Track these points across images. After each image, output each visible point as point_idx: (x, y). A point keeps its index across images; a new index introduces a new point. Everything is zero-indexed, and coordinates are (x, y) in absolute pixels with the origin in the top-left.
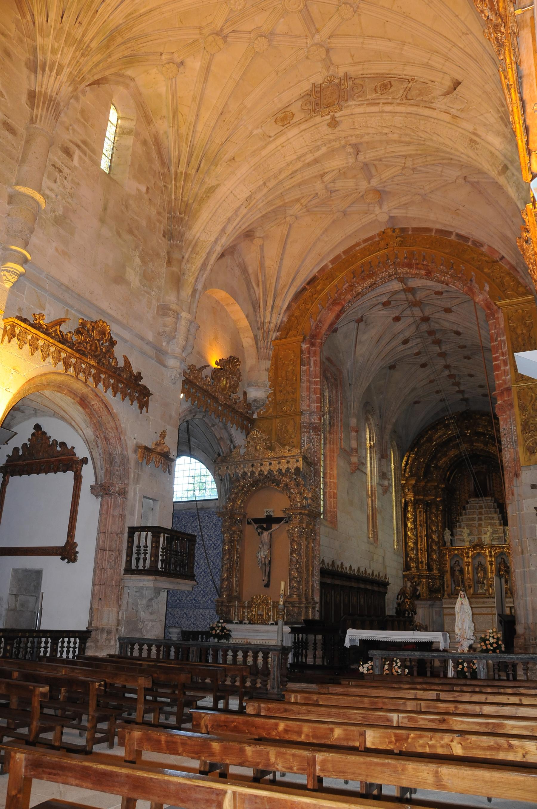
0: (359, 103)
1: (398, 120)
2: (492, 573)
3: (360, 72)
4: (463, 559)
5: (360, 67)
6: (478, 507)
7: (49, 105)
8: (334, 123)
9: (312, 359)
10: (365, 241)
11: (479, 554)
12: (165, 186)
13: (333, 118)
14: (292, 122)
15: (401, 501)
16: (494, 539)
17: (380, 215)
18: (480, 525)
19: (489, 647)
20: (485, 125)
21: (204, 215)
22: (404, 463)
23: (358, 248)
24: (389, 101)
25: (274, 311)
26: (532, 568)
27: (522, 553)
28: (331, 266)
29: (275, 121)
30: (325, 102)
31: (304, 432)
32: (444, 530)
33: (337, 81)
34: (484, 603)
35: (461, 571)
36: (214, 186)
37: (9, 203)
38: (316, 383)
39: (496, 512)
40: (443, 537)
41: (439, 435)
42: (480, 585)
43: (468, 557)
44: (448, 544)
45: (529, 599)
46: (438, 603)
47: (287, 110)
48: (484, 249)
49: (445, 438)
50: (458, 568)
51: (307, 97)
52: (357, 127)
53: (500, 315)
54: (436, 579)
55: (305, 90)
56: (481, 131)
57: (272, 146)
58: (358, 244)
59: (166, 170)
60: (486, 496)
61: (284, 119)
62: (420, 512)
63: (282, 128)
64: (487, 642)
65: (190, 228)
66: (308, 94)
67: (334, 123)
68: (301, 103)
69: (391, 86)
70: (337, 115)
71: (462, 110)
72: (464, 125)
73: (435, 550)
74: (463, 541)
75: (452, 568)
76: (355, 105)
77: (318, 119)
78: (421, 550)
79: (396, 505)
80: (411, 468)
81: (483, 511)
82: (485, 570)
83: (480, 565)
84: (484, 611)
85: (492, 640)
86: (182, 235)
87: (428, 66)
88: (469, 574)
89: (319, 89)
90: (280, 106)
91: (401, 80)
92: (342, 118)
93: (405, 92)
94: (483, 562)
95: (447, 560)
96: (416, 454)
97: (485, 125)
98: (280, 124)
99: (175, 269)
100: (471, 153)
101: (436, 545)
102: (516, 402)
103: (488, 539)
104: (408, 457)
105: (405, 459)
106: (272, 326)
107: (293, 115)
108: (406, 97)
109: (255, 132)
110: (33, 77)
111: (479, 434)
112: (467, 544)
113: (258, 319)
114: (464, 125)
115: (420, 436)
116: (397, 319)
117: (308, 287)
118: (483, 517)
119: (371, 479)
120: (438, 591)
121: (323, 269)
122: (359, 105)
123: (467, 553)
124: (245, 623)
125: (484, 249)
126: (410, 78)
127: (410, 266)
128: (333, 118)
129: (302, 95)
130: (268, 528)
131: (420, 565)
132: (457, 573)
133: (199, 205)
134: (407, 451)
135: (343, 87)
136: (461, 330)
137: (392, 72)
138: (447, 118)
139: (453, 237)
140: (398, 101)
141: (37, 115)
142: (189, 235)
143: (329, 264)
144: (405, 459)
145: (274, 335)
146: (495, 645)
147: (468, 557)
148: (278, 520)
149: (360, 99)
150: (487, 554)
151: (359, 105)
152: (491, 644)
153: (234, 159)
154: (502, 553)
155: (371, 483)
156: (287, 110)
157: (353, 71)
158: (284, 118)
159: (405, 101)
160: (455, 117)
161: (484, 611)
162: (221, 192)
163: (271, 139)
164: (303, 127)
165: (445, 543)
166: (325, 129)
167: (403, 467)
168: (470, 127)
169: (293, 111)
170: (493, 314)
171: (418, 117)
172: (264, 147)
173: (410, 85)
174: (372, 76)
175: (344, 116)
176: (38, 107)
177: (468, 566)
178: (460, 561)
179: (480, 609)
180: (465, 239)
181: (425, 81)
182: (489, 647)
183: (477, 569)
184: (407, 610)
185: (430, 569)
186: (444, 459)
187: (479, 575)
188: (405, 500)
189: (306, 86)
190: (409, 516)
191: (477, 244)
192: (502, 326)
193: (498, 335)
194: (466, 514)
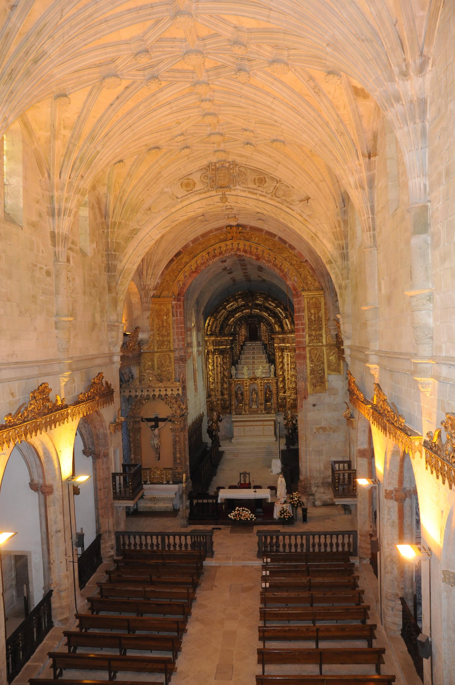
0: (243, 189)
3: (244, 163)
5: (244, 159)
7: (65, 241)
8: (224, 199)
9: (178, 311)
10: (217, 229)
12: (103, 232)
13: (224, 194)
14: (194, 190)
15: (205, 351)
16: (263, 373)
18: (254, 362)
19: (295, 502)
21: (130, 250)
22: (206, 325)
23: (211, 234)
24: (264, 194)
25: (153, 277)
26: (311, 449)
27: (306, 440)
28: (191, 245)
29: (181, 185)
30: (220, 182)
31: (176, 363)
33: (227, 165)
36: (136, 229)
37: (56, 328)
38: (181, 328)
39: (263, 353)
41: (232, 305)
44: (234, 377)
47: (190, 177)
48: (296, 251)
49: (234, 307)
50: (240, 392)
51: (204, 171)
52: (239, 202)
55: (203, 164)
56: (320, 235)
59: (103, 219)
61: (187, 185)
62: (217, 357)
63: (187, 193)
64: (294, 500)
65: (121, 261)
66: (205, 168)
67: (224, 199)
68: (200, 174)
69: (265, 182)
70: (227, 193)
71: (310, 216)
72: (310, 227)
74: (243, 374)
76: (241, 190)
77: (214, 193)
80: (211, 328)
83: (254, 390)
85: (296, 499)
86: (115, 266)
89: (214, 167)
90: (184, 173)
91: (273, 179)
92: (230, 196)
93: (275, 191)
98: (185, 189)
99: (114, 295)
102: (308, 356)
104: (209, 321)
106: (151, 287)
107: (195, 184)
108: (275, 194)
109: (166, 190)
110: (51, 220)
111: (257, 305)
113: (142, 283)
117: (175, 259)
118: (256, 356)
120: (227, 408)
121: (186, 247)
122: (243, 191)
124: (149, 484)
126: (278, 179)
128: (224, 194)
129: (201, 167)
130: (156, 426)
132: (239, 395)
133: (126, 242)
135: (232, 171)
137: (267, 170)
139: (276, 239)
140: (270, 196)
141: (58, 252)
142: (120, 267)
143: (190, 243)
144: (207, 321)
145: (151, 294)
146: (298, 501)
148: (164, 420)
149: (244, 186)
151: (243, 191)
152: (296, 501)
153: (150, 209)
156: (190, 177)
157: (239, 160)
158: (187, 184)
159: (274, 197)
162: (141, 235)
163: (179, 200)
164: (203, 196)
165: (232, 376)
166: (217, 199)
168: (314, 230)
169: (195, 180)
171: (281, 211)
172: (174, 206)
173: (278, 185)
174: (253, 168)
175: (232, 195)
176: (58, 246)
181: (288, 185)
182: (295, 502)
183: (252, 393)
185: (222, 394)
186: (232, 319)
189: (205, 162)
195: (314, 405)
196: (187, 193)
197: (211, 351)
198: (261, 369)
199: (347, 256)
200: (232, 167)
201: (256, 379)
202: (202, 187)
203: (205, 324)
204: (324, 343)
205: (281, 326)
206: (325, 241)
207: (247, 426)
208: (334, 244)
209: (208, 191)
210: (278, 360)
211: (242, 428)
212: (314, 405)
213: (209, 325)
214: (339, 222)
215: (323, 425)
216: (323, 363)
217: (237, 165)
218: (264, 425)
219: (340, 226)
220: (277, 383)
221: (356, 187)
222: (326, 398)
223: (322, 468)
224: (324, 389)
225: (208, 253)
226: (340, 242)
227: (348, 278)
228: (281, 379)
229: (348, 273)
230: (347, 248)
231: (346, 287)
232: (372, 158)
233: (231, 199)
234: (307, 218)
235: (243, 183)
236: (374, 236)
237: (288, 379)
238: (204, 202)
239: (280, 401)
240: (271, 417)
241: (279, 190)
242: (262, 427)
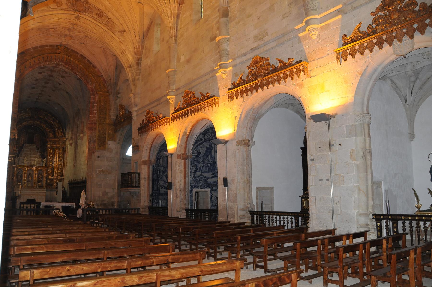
1: (101, 30)
4: (22, 171)
8: (78, 18)
11: (30, 169)
14: (61, 7)
17: (65, 41)
18: (31, 157)
20: (129, 50)
34: (34, 190)
35: (21, 176)
43: (25, 170)
45: (92, 192)
48: (96, 70)
50: (20, 175)
53: (96, 96)
56: (127, 51)
57: (51, 13)
58: (46, 46)
63: (56, 7)
67: (78, 18)
72: (122, 46)
74: (24, 163)
75: (17, 174)
77: (73, 13)
82: (32, 177)
83: (30, 174)
84: (35, 194)
87: (118, 20)
91: (106, 16)
94: (31, 173)
97: (129, 50)
100: (121, 55)
103: (35, 163)
114: (122, 46)
116: (40, 73)
125: (96, 70)
127: (66, 63)
136: (61, 83)
138: (118, 40)
139: (86, 60)
147: (25, 170)
154: (41, 170)
160: (120, 42)
161: (35, 194)
164: (66, 12)
166: (73, 17)
168: (124, 48)
170: (94, 95)
177: (25, 174)
180: (90, 63)
191: (94, 67)
192: (97, 100)
193: (94, 103)
194: (23, 151)
195: (99, 157)
196: (56, 7)
198: (36, 161)
199: (141, 64)
200: (85, 2)
201: (32, 166)
202: (66, 7)
204: (107, 122)
205: (54, 134)
206: (129, 55)
208: (133, 57)
209: (70, 10)
210: (49, 156)
212: (99, 157)
214: (139, 46)
215: (103, 169)
216: (105, 133)
217: (88, 3)
219: (139, 48)
220: (47, 170)
221: (171, 17)
222: (106, 154)
223: (101, 195)
224: (105, 149)
225: (43, 58)
226: (138, 56)
227: (140, 75)
228: (50, 167)
229: (140, 72)
230: (141, 60)
231: (138, 79)
232: (180, 5)
233: (82, 20)
234: (122, 41)
235: (90, 13)
236: (176, 40)
237: (56, 167)
238: (66, 15)
239: (49, 181)
241: (109, 24)
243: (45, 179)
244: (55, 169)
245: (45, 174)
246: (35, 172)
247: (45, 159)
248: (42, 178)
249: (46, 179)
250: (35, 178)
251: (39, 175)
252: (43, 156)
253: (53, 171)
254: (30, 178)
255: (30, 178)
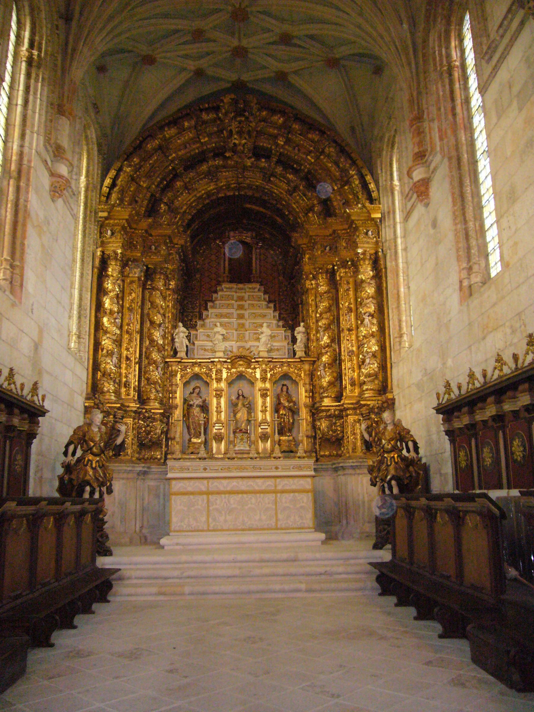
2: (264, 411)
4: (207, 384)
6: (235, 298)
11: (241, 376)
22: (108, 181)
32: (175, 327)
34: (254, 468)
35: (205, 408)
40: (173, 339)
42: (239, 435)
43: (219, 380)
44: (182, 354)
46: (155, 468)
50: (198, 402)
54: (154, 420)
60: (249, 281)
73: (155, 362)
78: (128, 359)
79: (85, 218)
81: (246, 304)
82: (250, 408)
84: (259, 484)
88: (219, 412)
95: (177, 385)
96: (137, 168)
101: (159, 351)
104: (120, 170)
105: (112, 173)
112: (221, 354)
115: (147, 134)
119: (23, 136)
120: (155, 444)
123: (219, 372)
131: (123, 390)
132: (196, 411)
134: (118, 158)
144: (112, 173)
147: (219, 380)
150: (258, 375)
154: (286, 376)
155: (22, 146)
161: (259, 484)
165: (176, 353)
167: (105, 190)
178: (203, 389)
179: (251, 482)
183: (236, 405)
184: (88, 483)
185: (142, 400)
187: (239, 415)
188: (103, 252)
190: (109, 285)
197: (116, 254)
198: (266, 335)
201: (246, 359)
203: (103, 181)
207: (219, 493)
210: (317, 306)
211: (201, 501)
213: (113, 185)
218: (275, 492)
220: (312, 375)
239: (323, 425)
240: (300, 468)
242: (272, 497)
243: (304, 414)
244: (346, 365)
245: (302, 395)
246: (259, 385)
247: (301, 329)
248: (294, 411)
249: (313, 415)
250: (264, 412)
251: (278, 397)
252: (290, 311)
253: (339, 377)
254: (242, 415)
255: (242, 415)
